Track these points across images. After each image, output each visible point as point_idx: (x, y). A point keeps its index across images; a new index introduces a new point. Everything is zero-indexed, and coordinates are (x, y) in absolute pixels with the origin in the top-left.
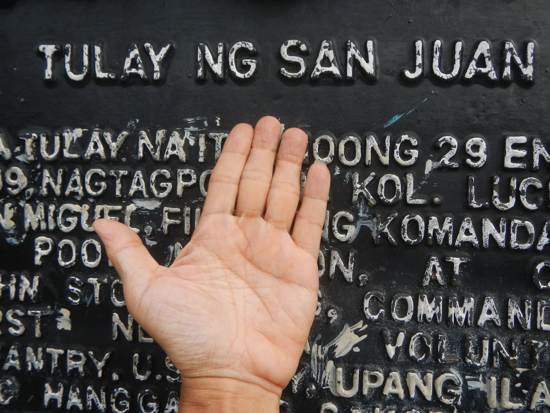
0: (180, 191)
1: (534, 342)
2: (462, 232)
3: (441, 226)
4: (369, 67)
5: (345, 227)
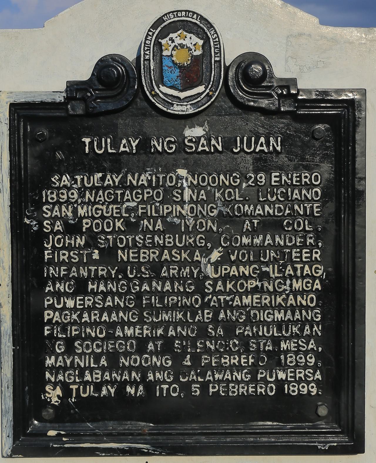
0: (145, 199)
1: (285, 250)
2: (257, 210)
3: (249, 208)
4: (220, 148)
5: (213, 210)
